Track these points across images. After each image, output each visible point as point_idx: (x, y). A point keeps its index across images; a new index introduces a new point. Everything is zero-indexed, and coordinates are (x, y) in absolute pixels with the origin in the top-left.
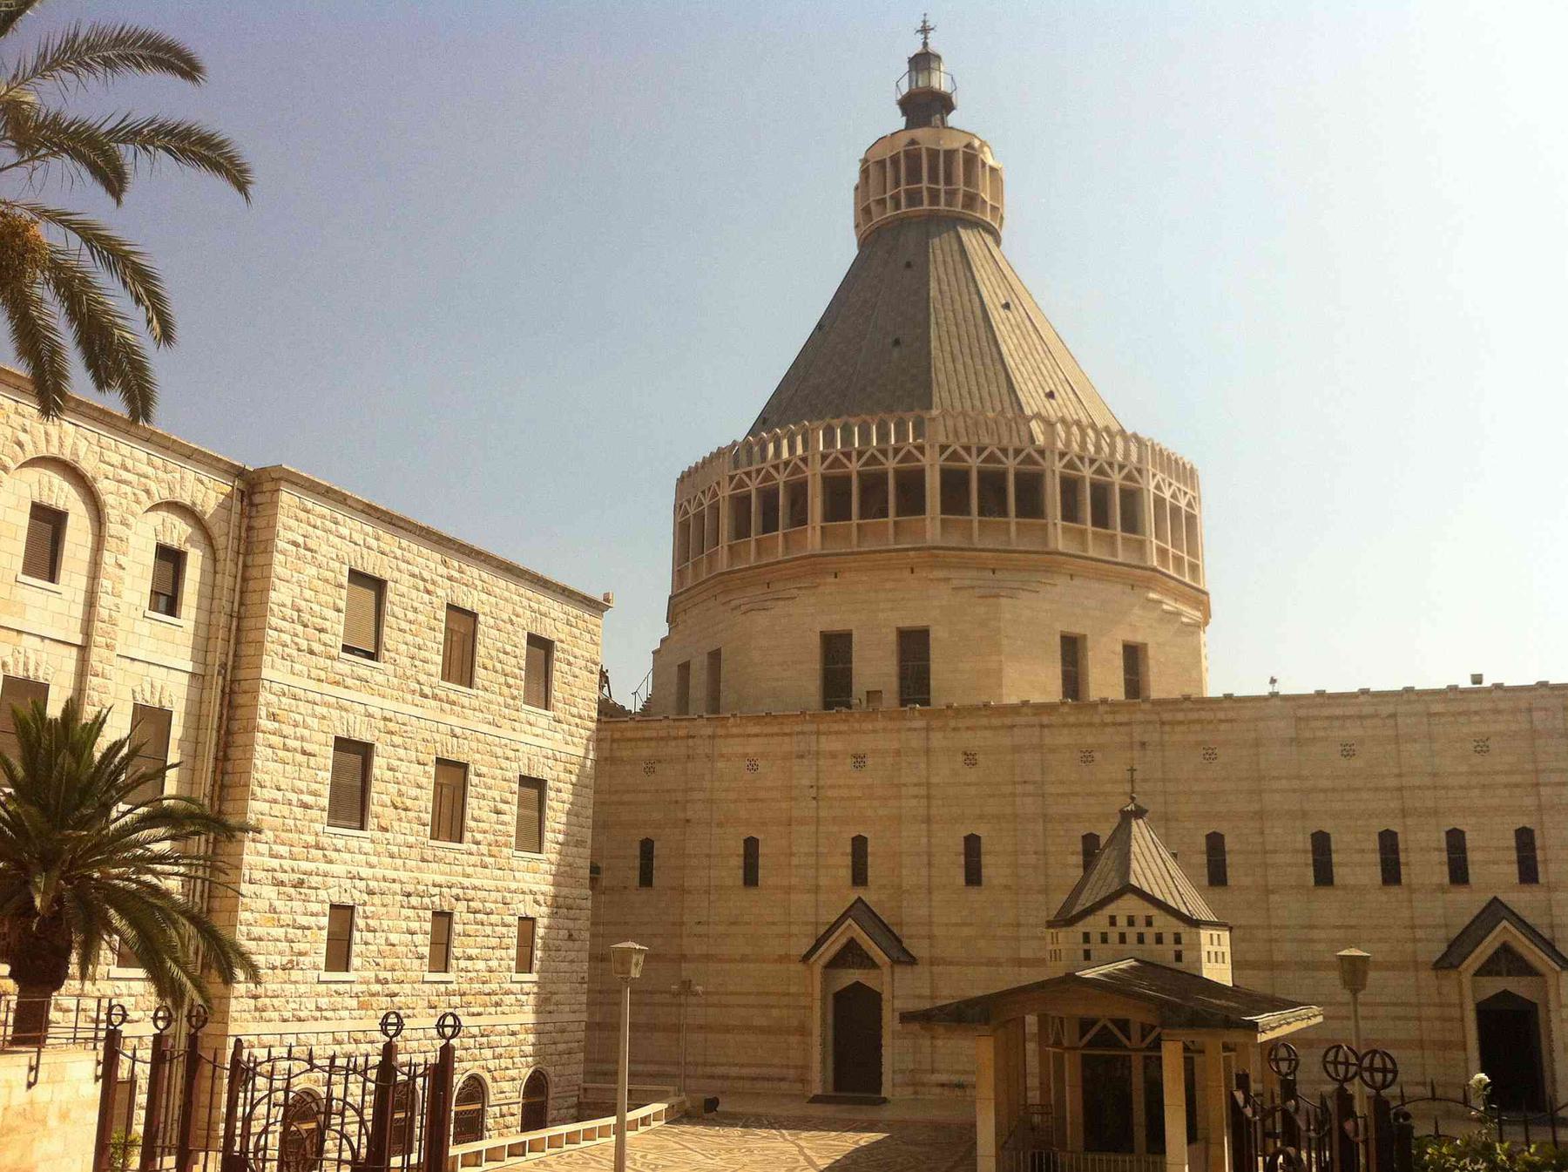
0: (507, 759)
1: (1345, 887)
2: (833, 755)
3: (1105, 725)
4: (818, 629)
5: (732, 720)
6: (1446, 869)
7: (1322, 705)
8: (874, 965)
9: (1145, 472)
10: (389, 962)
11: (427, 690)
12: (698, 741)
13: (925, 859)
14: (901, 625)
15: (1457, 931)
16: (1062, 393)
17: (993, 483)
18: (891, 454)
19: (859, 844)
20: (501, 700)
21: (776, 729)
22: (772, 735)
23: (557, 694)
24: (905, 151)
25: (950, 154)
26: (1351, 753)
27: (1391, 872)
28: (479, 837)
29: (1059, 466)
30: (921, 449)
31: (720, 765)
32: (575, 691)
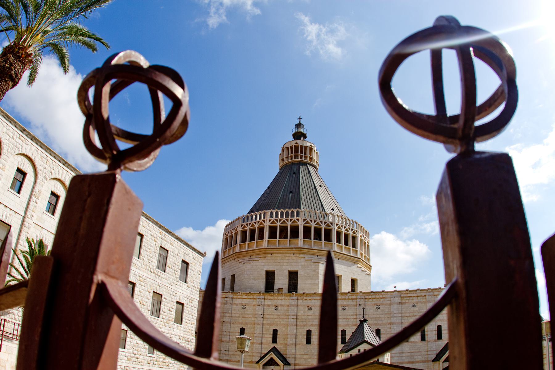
0: (173, 295)
2: (269, 306)
3: (349, 299)
4: (265, 269)
5: (238, 294)
6: (437, 335)
7: (407, 294)
8: (278, 365)
10: (137, 349)
11: (152, 271)
12: (228, 299)
13: (295, 336)
14: (290, 270)
15: (438, 352)
16: (335, 209)
17: (318, 231)
18: (289, 221)
19: (275, 332)
20: (173, 277)
21: (252, 297)
22: (250, 299)
23: (189, 279)
24: (294, 145)
25: (306, 147)
26: (414, 306)
28: (164, 317)
29: (336, 228)
30: (298, 220)
31: (234, 306)
32: (194, 279)
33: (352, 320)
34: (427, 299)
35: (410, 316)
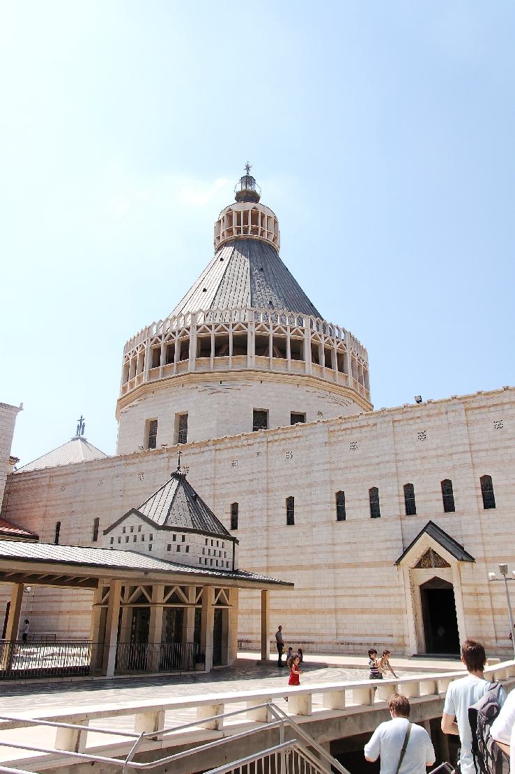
1: (351, 521)
3: (243, 446)
6: (404, 507)
12: (80, 473)
25: (246, 213)
27: (375, 513)
33: (247, 483)
35: (347, 468)
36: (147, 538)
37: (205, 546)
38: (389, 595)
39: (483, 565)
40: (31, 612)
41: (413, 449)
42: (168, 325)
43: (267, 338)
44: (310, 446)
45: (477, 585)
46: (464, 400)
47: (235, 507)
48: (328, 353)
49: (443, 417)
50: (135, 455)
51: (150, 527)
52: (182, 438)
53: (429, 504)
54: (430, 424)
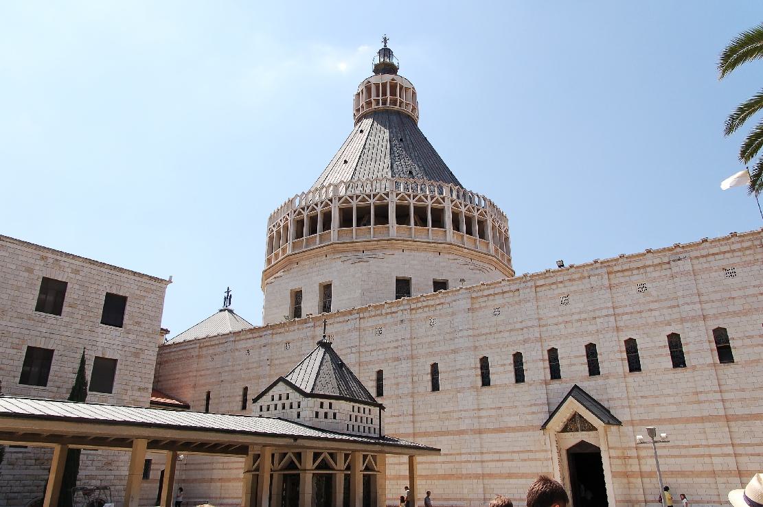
1: (495, 386)
3: (387, 314)
6: (548, 371)
7: (484, 290)
9: (446, 199)
25: (384, 85)
27: (520, 377)
29: (396, 200)
34: (522, 297)
35: (490, 333)
36: (295, 406)
37: (352, 413)
38: (536, 460)
39: (631, 428)
40: (184, 480)
41: (556, 313)
42: (310, 196)
43: (408, 207)
44: (453, 314)
45: (625, 449)
46: (606, 263)
47: (380, 374)
48: (469, 221)
49: (587, 280)
50: (281, 325)
51: (297, 394)
52: (326, 307)
53: (574, 368)
54: (573, 288)
